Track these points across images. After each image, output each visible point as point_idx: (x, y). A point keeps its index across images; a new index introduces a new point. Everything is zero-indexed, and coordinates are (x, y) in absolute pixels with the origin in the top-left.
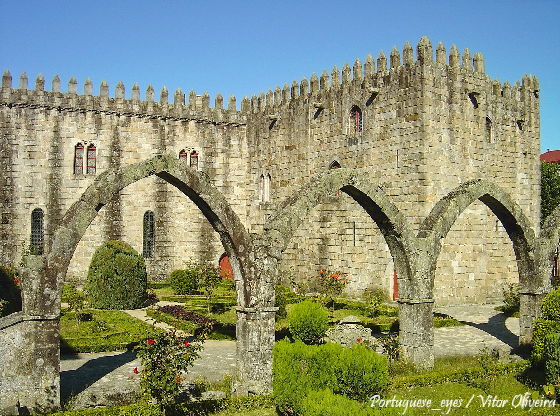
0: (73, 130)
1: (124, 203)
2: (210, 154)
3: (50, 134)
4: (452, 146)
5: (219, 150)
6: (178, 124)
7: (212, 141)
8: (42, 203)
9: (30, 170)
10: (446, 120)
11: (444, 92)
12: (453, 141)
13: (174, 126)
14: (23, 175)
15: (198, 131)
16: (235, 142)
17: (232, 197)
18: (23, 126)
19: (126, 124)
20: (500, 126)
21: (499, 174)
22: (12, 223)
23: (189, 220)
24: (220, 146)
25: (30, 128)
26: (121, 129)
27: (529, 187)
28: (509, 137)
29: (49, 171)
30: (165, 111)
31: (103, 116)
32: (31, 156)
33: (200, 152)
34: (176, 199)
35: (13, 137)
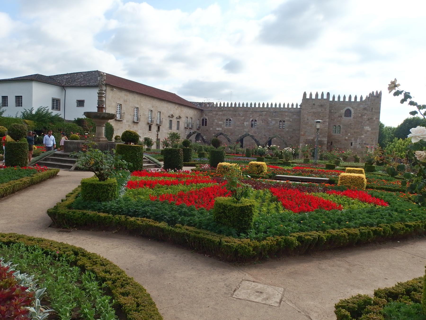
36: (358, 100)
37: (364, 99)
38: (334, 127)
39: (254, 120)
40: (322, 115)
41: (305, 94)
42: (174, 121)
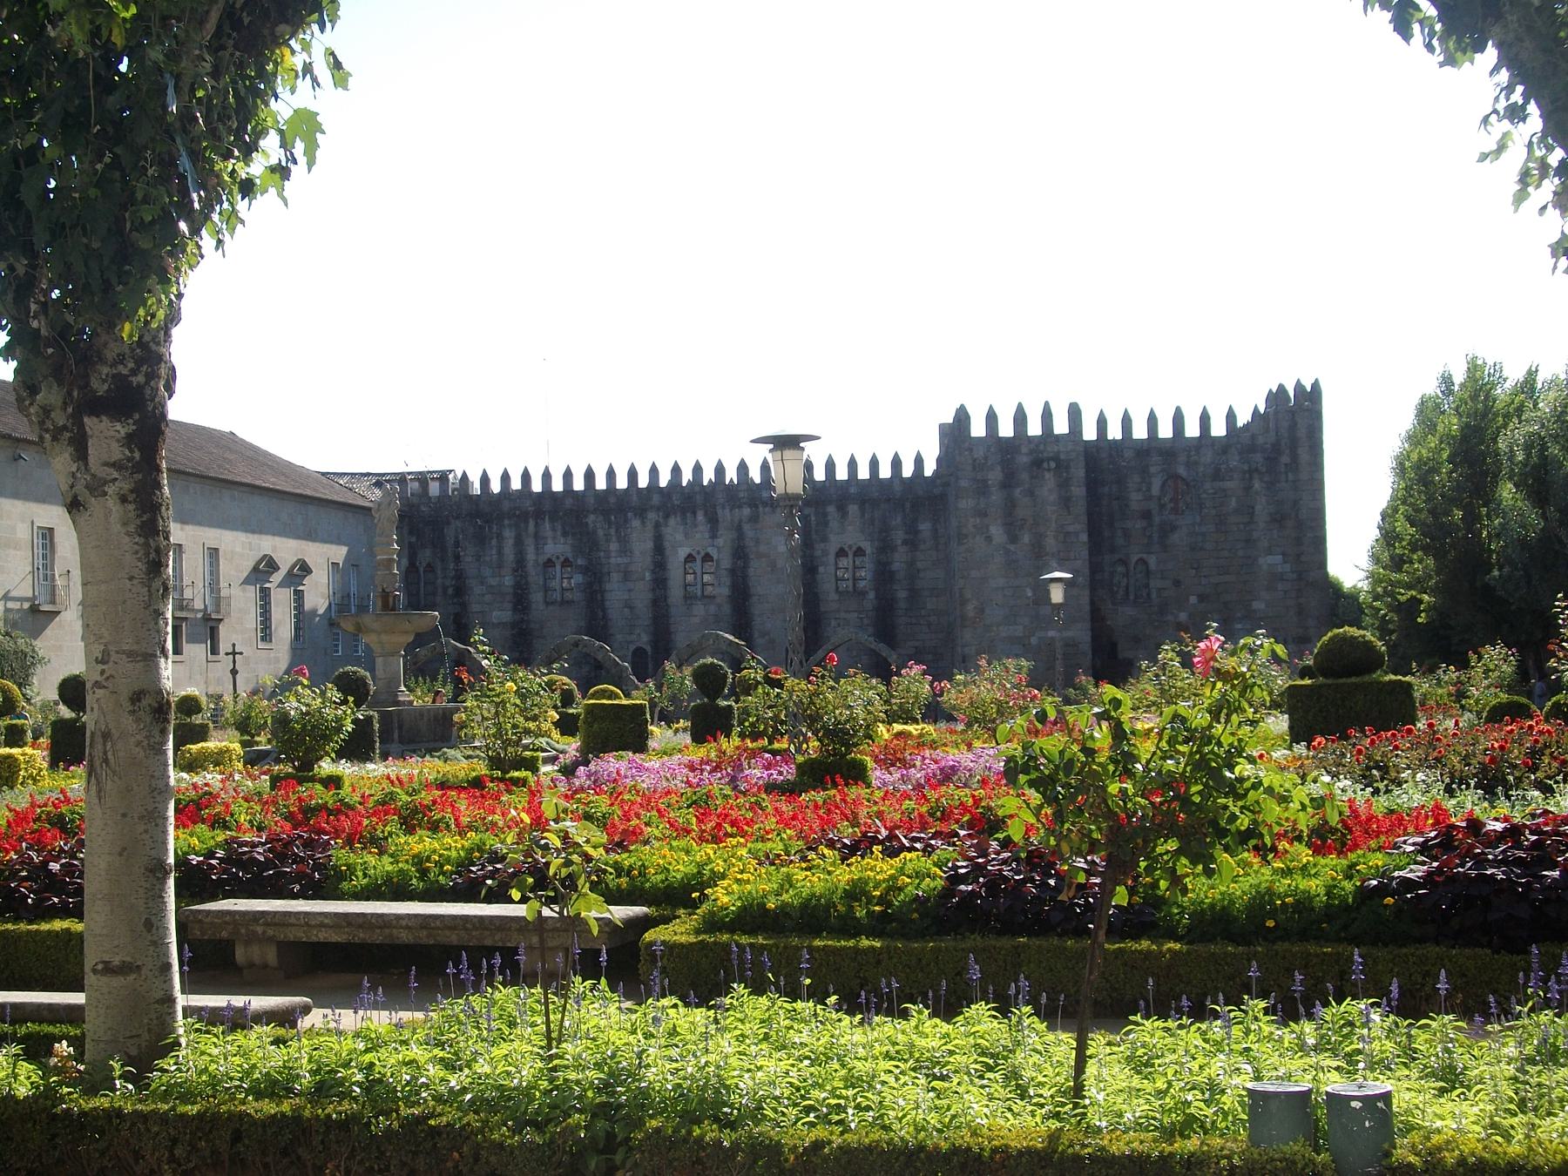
0: (679, 537)
2: (885, 547)
3: (650, 545)
4: (1012, 547)
5: (899, 542)
6: (831, 509)
9: (626, 597)
11: (995, 476)
13: (825, 515)
15: (863, 515)
16: (925, 527)
17: (923, 612)
18: (614, 539)
19: (754, 519)
23: (855, 653)
24: (899, 536)
25: (624, 542)
26: (746, 527)
27: (1295, 576)
28: (1234, 499)
29: (650, 596)
31: (719, 511)
33: (868, 547)
34: (833, 623)
35: (602, 554)
36: (1218, 429)
37: (1243, 418)
40: (1054, 517)
41: (962, 417)
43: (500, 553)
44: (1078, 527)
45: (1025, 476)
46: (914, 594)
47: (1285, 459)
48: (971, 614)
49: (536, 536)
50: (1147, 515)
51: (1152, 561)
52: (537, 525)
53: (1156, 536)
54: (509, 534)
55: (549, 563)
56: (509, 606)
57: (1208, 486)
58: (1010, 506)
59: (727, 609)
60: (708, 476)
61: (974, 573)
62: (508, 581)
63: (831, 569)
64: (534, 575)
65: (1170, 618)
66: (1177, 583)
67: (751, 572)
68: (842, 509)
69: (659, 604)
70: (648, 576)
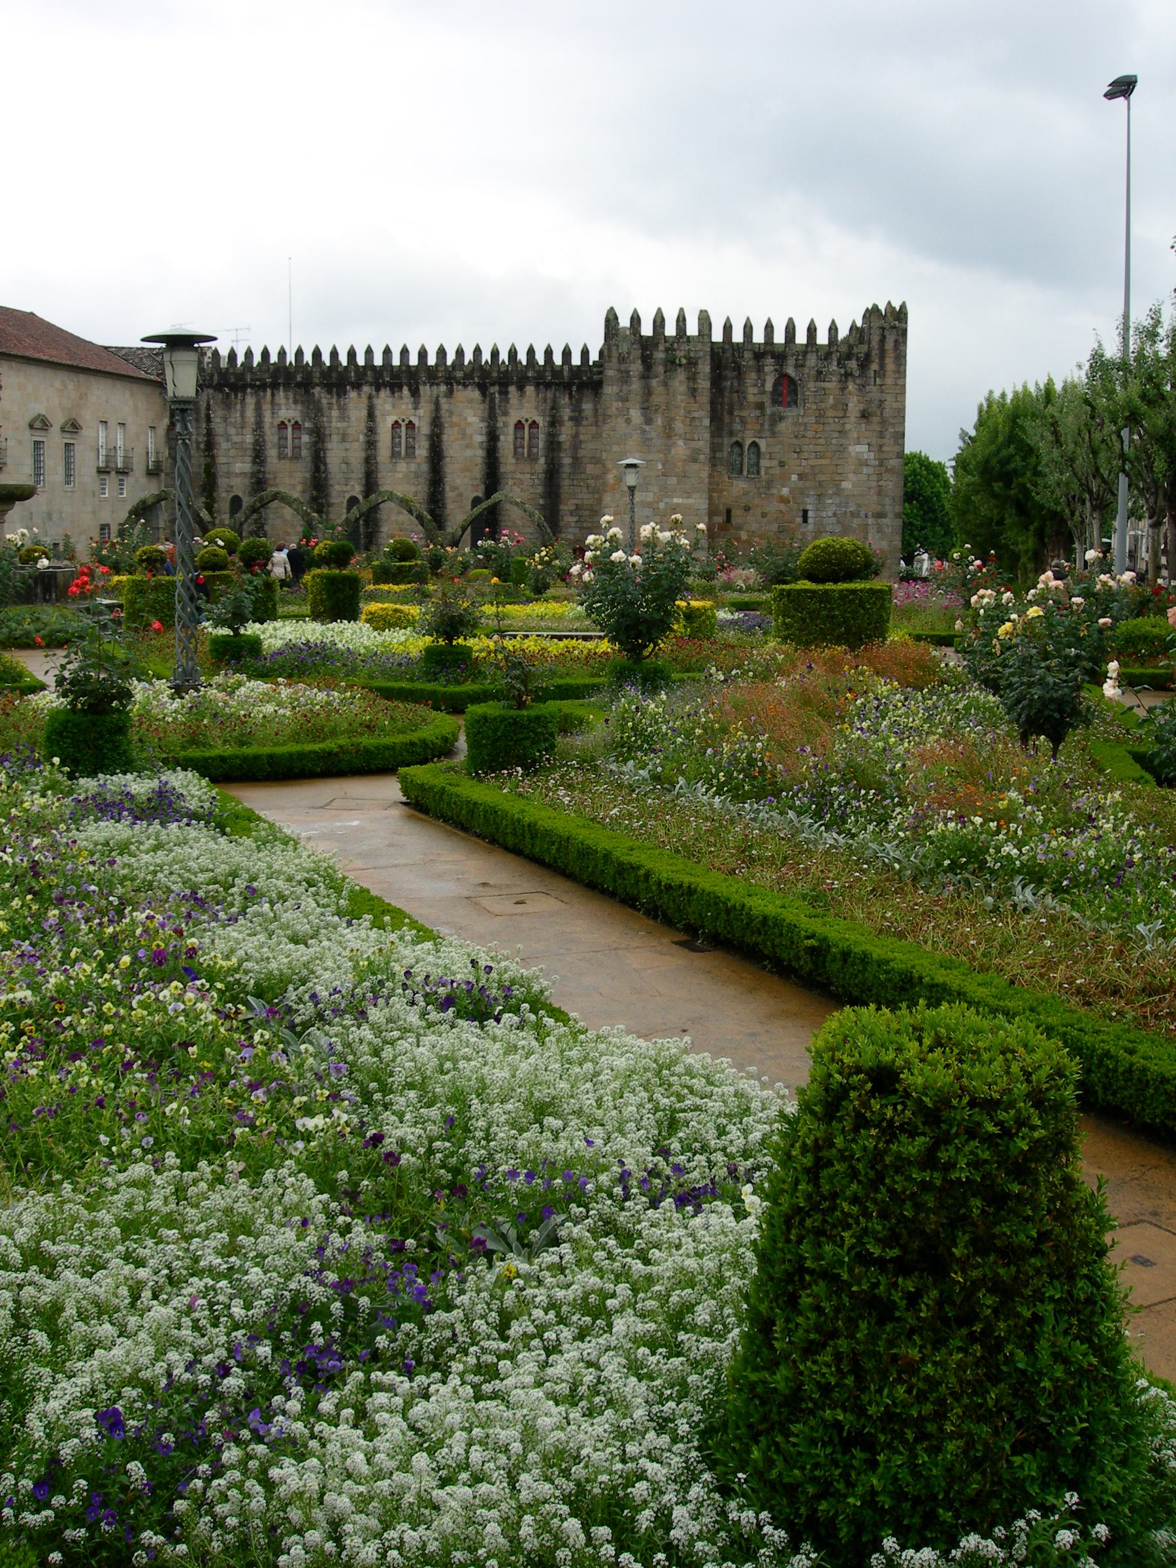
0: (388, 407)
1: (447, 488)
2: (554, 422)
3: (364, 413)
4: (647, 428)
6: (512, 389)
7: (554, 407)
8: (356, 489)
10: (639, 398)
11: (636, 368)
12: (649, 421)
13: (507, 393)
14: (338, 461)
16: (587, 407)
19: (450, 393)
20: (811, 385)
21: (805, 448)
22: (328, 513)
24: (566, 413)
25: (343, 409)
26: (443, 401)
29: (363, 455)
30: (495, 375)
32: (344, 438)
34: (511, 482)
36: (822, 339)
37: (843, 333)
38: (737, 450)
39: (403, 425)
42: (55, 440)
43: (243, 416)
44: (702, 413)
45: (660, 369)
46: (577, 461)
47: (874, 366)
48: (612, 481)
49: (273, 403)
50: (760, 406)
51: (763, 444)
52: (273, 395)
53: (766, 426)
54: (250, 401)
55: (282, 426)
56: (249, 459)
57: (811, 385)
58: (648, 393)
59: (425, 467)
60: (291, 358)
61: (615, 448)
62: (249, 439)
63: (511, 438)
64: (271, 436)
65: (774, 491)
66: (782, 464)
67: (445, 438)
68: (521, 388)
69: (370, 461)
70: (362, 438)
